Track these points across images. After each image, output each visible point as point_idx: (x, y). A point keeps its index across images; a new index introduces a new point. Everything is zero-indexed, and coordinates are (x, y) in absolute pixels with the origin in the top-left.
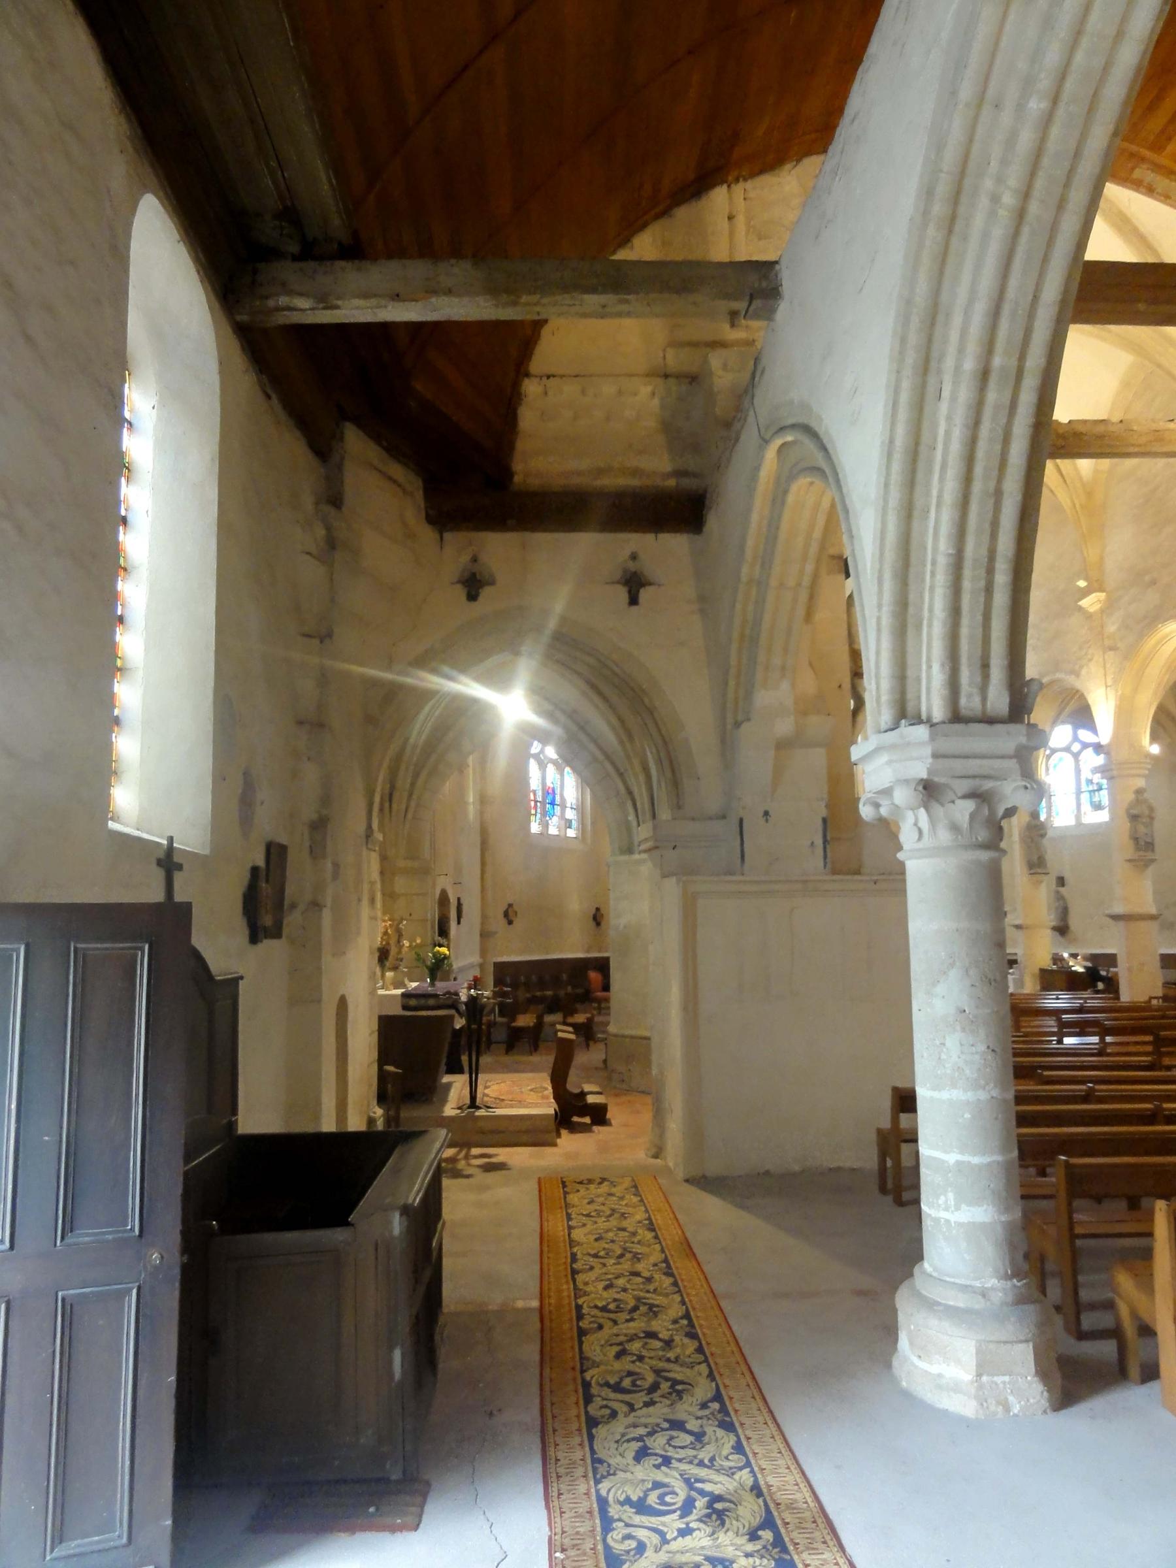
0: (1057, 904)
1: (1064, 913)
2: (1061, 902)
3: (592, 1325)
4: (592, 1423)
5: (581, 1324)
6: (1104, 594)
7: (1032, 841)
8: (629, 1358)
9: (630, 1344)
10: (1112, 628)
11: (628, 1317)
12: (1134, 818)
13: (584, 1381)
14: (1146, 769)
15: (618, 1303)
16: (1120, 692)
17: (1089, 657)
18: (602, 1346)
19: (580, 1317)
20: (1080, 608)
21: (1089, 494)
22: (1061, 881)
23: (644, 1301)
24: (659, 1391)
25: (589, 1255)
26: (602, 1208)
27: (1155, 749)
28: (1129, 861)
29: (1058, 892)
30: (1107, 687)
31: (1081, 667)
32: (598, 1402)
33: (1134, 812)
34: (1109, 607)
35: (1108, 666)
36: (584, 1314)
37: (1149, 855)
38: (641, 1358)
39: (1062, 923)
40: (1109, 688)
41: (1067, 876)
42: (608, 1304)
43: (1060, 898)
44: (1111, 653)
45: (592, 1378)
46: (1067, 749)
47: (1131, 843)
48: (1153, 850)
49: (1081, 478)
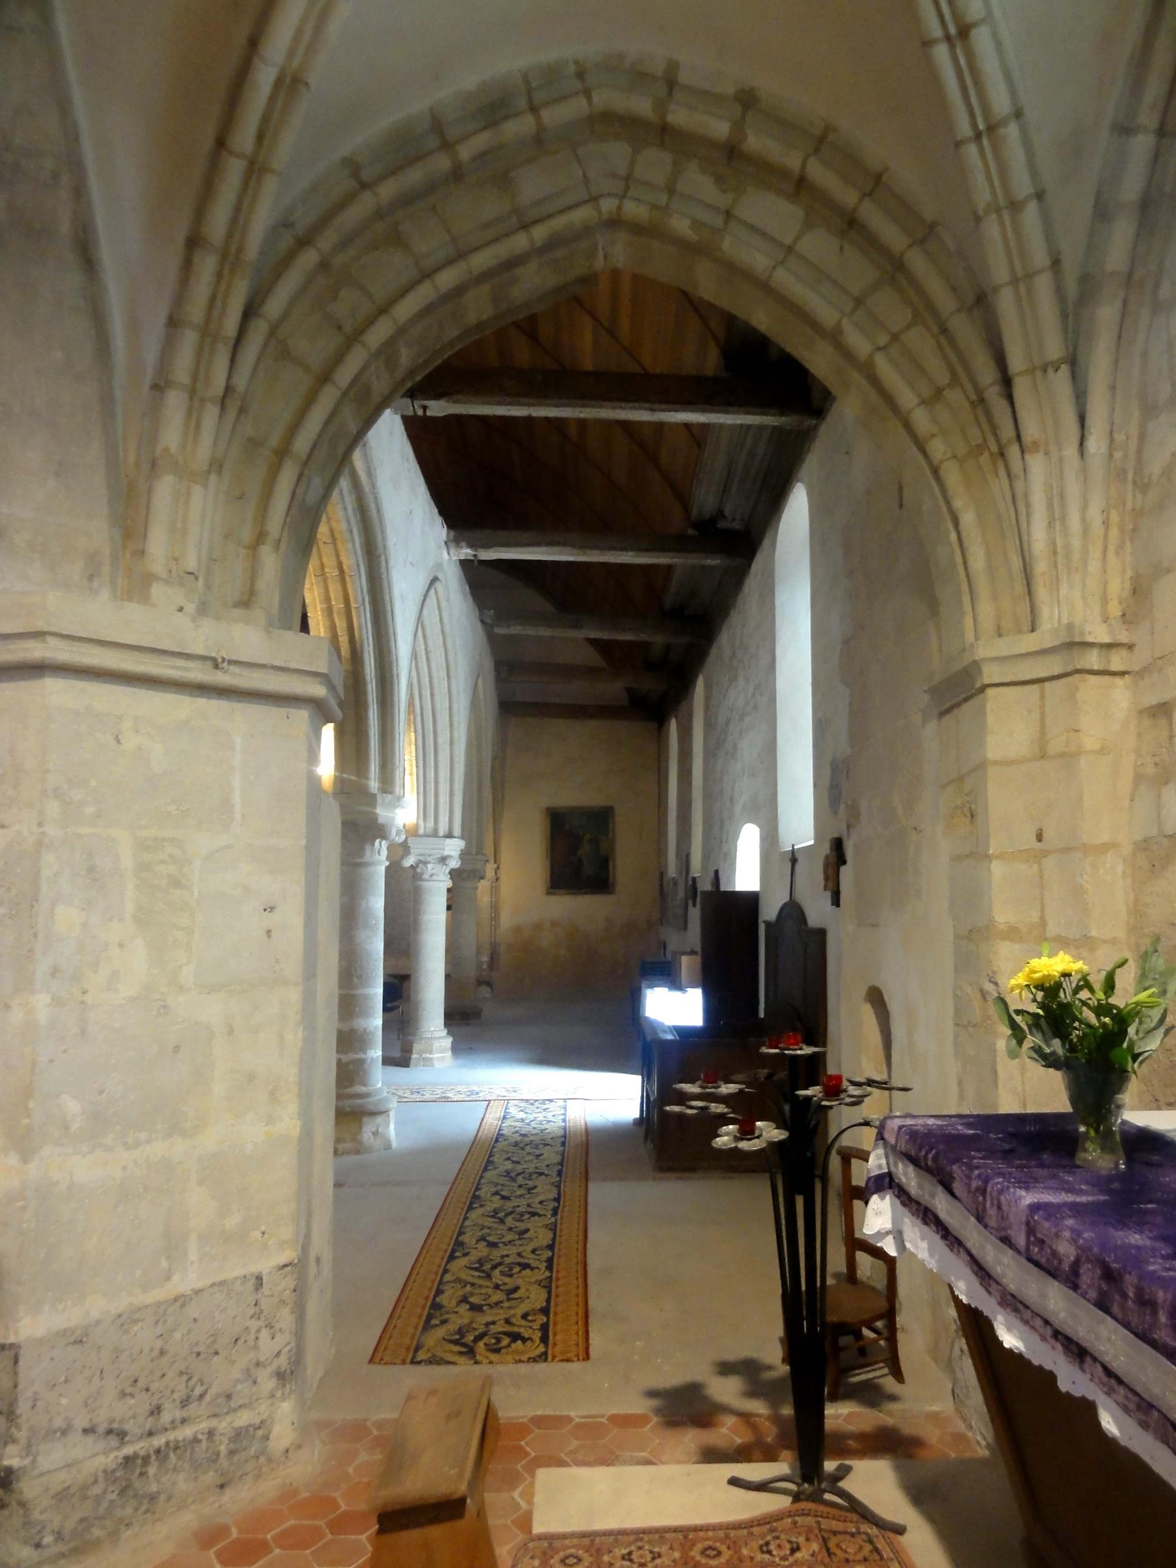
3: (534, 1318)
4: (564, 1136)
5: (545, 1319)
8: (507, 1287)
9: (501, 1299)
11: (492, 1326)
13: (547, 1345)
15: (510, 1273)
18: (537, 1237)
19: (550, 1261)
23: (463, 1349)
24: (477, 1334)
25: (540, 1216)
26: (540, 1106)
32: (536, 1326)
36: (546, 1261)
38: (497, 1287)
42: (520, 1272)
45: (544, 1273)
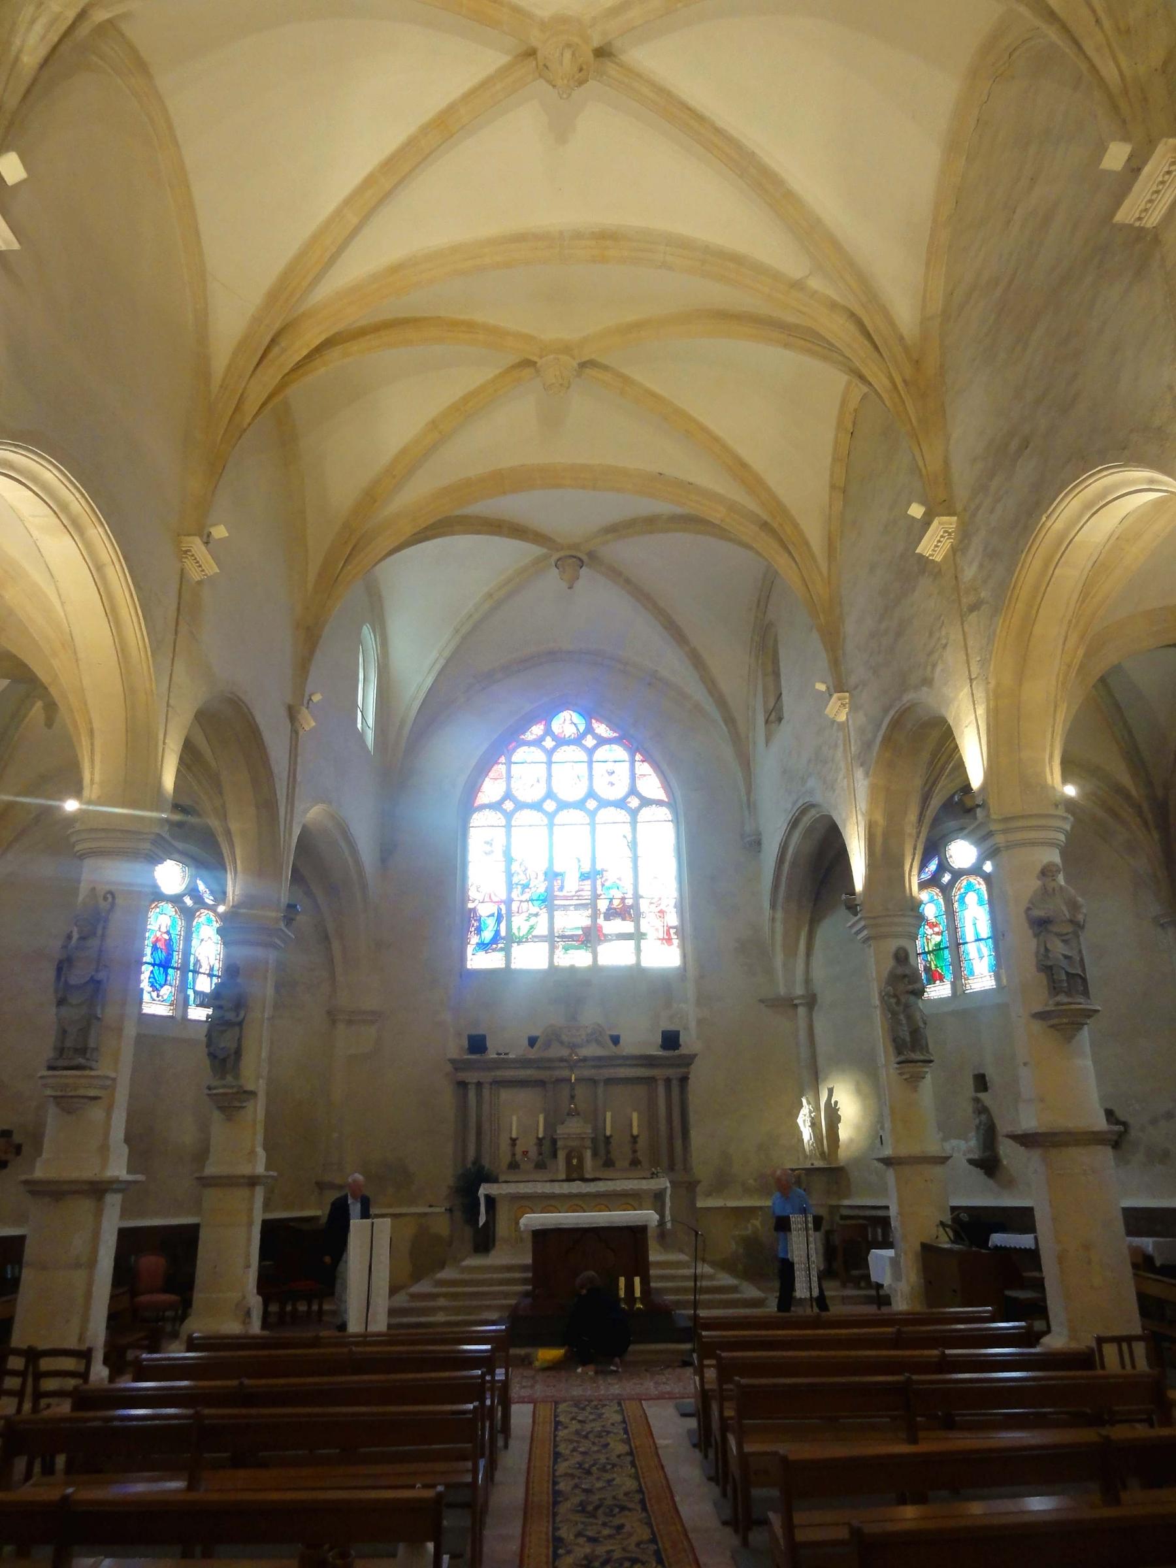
0: (977, 1121)
1: (989, 1135)
2: (984, 1117)
6: (955, 519)
7: (898, 1003)
10: (969, 572)
12: (1041, 925)
14: (1059, 829)
16: (993, 683)
17: (944, 641)
20: (923, 561)
21: (917, 364)
22: (981, 1082)
27: (1070, 791)
28: (1041, 1016)
29: (977, 1100)
30: (971, 680)
31: (934, 666)
33: (1038, 913)
34: (964, 536)
35: (970, 643)
37: (1082, 1003)
39: (987, 1154)
40: (974, 683)
41: (991, 1073)
43: (982, 1110)
44: (973, 617)
46: (976, 870)
47: (1042, 978)
48: (1086, 993)
49: (901, 338)
